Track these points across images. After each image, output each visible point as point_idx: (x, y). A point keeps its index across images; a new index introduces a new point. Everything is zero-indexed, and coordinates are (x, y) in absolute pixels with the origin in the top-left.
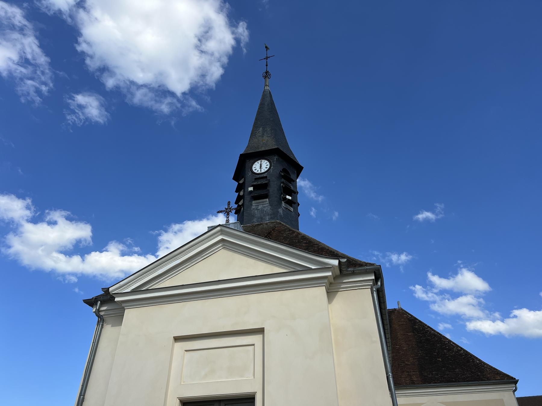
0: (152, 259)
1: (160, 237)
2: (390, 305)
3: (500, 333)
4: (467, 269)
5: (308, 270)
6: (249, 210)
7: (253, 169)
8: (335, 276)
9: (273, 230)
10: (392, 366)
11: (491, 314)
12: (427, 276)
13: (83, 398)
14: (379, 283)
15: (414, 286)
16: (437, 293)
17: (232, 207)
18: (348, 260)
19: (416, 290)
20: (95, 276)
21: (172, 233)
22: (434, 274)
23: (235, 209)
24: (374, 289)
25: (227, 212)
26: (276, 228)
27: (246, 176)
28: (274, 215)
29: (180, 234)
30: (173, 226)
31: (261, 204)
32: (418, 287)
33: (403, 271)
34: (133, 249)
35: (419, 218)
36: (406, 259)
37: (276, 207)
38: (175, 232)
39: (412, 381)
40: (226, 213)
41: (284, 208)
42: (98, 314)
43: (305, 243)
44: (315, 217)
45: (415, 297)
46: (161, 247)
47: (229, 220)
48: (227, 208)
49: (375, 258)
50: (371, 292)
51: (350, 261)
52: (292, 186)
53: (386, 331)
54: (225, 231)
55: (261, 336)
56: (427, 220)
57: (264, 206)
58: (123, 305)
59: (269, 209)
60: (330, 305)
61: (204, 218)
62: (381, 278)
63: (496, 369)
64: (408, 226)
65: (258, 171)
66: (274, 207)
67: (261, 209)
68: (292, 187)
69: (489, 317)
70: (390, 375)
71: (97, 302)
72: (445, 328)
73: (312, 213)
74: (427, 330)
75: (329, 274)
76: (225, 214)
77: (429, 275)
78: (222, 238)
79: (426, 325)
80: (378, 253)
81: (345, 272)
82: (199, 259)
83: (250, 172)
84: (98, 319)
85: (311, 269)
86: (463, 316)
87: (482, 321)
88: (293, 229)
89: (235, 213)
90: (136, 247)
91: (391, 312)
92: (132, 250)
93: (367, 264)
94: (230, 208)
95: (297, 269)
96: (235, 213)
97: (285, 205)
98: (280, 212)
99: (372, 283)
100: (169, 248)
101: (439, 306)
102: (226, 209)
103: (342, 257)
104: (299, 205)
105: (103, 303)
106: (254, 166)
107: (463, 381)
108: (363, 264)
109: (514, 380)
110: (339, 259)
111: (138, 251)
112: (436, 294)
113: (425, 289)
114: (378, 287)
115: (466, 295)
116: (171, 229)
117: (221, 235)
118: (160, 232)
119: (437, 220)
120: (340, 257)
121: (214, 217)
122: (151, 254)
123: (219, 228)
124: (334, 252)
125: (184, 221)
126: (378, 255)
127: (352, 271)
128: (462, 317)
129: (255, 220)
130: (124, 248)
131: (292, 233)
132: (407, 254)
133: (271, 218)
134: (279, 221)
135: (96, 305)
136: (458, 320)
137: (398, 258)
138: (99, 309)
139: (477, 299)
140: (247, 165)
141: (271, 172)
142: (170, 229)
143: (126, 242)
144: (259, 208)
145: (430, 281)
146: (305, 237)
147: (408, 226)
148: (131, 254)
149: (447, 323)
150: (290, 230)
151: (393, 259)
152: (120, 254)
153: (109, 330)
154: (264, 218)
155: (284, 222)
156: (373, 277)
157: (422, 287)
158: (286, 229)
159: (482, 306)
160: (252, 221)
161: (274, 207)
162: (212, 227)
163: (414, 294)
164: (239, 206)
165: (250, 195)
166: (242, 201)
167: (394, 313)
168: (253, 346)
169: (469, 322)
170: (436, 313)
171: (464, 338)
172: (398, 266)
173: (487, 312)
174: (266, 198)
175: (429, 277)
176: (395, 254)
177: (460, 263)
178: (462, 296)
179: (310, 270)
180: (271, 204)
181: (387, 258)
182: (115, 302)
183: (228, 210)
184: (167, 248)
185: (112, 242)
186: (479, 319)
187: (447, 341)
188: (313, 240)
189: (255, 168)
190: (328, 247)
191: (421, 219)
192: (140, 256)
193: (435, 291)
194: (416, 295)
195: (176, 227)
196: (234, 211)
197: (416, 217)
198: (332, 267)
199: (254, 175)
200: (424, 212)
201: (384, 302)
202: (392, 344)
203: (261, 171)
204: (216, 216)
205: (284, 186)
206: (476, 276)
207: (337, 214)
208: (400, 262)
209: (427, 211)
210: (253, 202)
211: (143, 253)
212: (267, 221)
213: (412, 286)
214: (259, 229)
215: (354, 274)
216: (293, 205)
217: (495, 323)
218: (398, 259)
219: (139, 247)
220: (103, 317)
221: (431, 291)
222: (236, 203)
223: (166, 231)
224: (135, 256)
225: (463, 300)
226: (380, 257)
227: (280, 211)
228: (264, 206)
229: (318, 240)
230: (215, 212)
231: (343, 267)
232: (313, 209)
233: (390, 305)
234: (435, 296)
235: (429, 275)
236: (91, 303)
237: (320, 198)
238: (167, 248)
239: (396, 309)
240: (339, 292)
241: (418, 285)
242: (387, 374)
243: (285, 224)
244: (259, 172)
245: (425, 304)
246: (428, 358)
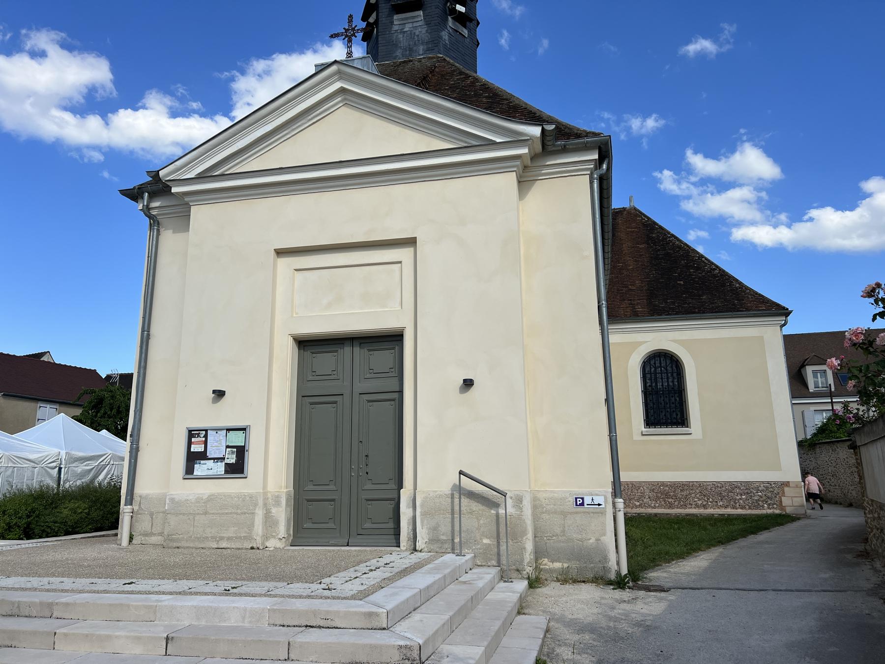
0: (224, 123)
1: (234, 84)
2: (618, 202)
3: (781, 244)
4: (752, 143)
5: (489, 144)
6: (388, 33)
8: (533, 155)
9: (431, 72)
10: (608, 293)
11: (773, 216)
12: (685, 154)
13: (148, 335)
14: (605, 166)
15: (661, 172)
16: (696, 182)
17: (356, 26)
18: (557, 128)
19: (663, 178)
20: (132, 152)
21: (254, 77)
22: (696, 152)
23: (362, 30)
24: (595, 176)
25: (348, 37)
26: (437, 70)
28: (434, 43)
29: (267, 79)
30: (255, 63)
31: (409, 21)
32: (667, 173)
33: (646, 147)
34: (189, 105)
35: (688, 51)
36: (654, 127)
37: (436, 27)
38: (259, 75)
39: (636, 312)
40: (347, 39)
41: (451, 30)
42: (148, 214)
43: (486, 97)
44: (508, 48)
45: (659, 190)
46: (237, 102)
47: (351, 52)
48: (347, 28)
49: (603, 125)
50: (590, 181)
51: (561, 128)
53: (606, 241)
54: (346, 72)
55: (412, 249)
56: (702, 56)
57: (415, 25)
58: (185, 199)
59: (424, 31)
60: (521, 202)
61: (308, 49)
62: (609, 157)
63: (762, 296)
64: (667, 67)
66: (432, 28)
67: (409, 32)
69: (769, 221)
70: (603, 304)
71: (143, 193)
72: (698, 237)
73: (503, 42)
74: (669, 240)
75: (525, 151)
76: (344, 39)
77: (689, 153)
78: (342, 87)
79: (669, 233)
80: (610, 116)
81: (550, 148)
82: (304, 123)
84: (150, 221)
85: (494, 143)
86: (730, 219)
87: (757, 226)
88: (468, 72)
89: (364, 39)
90: (195, 101)
91: (617, 213)
92: (188, 106)
93: (587, 134)
94: (353, 29)
95: (470, 144)
96: (364, 39)
97: (453, 23)
98: (444, 37)
99: (592, 166)
100: (251, 105)
101: (695, 204)
102: (347, 30)
103: (547, 122)
104: (478, 23)
105: (153, 195)
107: (709, 313)
108: (581, 134)
109: (787, 311)
110: (542, 125)
111: (199, 110)
112: (694, 184)
113: (675, 177)
114: (601, 173)
115: (741, 185)
116: (251, 70)
117: (340, 79)
118: (232, 74)
119: (719, 55)
120: (544, 121)
121: (325, 48)
122: (222, 115)
123: (334, 68)
124: (535, 113)
125: (273, 55)
126: (609, 119)
127: (562, 147)
128: (728, 221)
129: (399, 53)
130: (174, 104)
131: (465, 78)
132: (657, 118)
133: (428, 50)
134: (441, 56)
135: (143, 198)
136: (720, 226)
137: (642, 124)
138: (147, 206)
139: (758, 192)
142: (249, 68)
143: (176, 92)
144: (405, 30)
145: (689, 164)
146: (487, 86)
147: (667, 67)
148: (187, 113)
149: (701, 229)
150: (461, 73)
151: (633, 126)
152: (168, 113)
153: (169, 239)
154: (415, 48)
155: (450, 58)
156: (596, 156)
157: (674, 173)
158: (454, 71)
159: (763, 203)
160: (394, 55)
161: (432, 28)
162: (323, 64)
163: (659, 185)
164: (369, 24)
165: (389, 3)
166: (374, 15)
167: (622, 214)
168: (400, 265)
169: (736, 227)
170: (688, 215)
171: (723, 252)
172: (641, 137)
173: (769, 212)
174: (420, 10)
175: (687, 157)
176: (637, 118)
177: (743, 132)
178: (734, 188)
179: (492, 144)
180: (428, 24)
181: (623, 124)
182: (173, 194)
183: (350, 33)
184: (249, 104)
185: (150, 92)
186: (753, 223)
187: (698, 255)
188: (501, 91)
190: (526, 104)
191: (691, 54)
192: (203, 118)
193: (693, 179)
194: (662, 187)
195: (260, 65)
196: (360, 35)
197: (683, 50)
198: (530, 139)
200: (699, 40)
201: (609, 197)
202: (612, 261)
204: (329, 45)
206: (764, 155)
207: (546, 43)
208: (643, 131)
209: (705, 37)
210: (396, 17)
211: (208, 113)
212: (420, 55)
213: (657, 171)
214: (406, 70)
215: (564, 150)
216: (468, 23)
217: (778, 230)
218: (642, 126)
219: (199, 103)
220: (156, 218)
221: (687, 180)
222: (365, 18)
223: (243, 72)
224: (193, 117)
225: (736, 194)
226: (611, 123)
227: (445, 35)
228: (415, 25)
229: (508, 92)
230: (328, 38)
231: (548, 138)
232: (506, 33)
233: (618, 202)
234: (692, 187)
235: (689, 153)
236: (134, 195)
237: (518, 11)
238: (249, 104)
239: (626, 208)
240: (538, 181)
241: (668, 170)
242: (599, 303)
243: (452, 61)
245: (674, 200)
246: (663, 280)
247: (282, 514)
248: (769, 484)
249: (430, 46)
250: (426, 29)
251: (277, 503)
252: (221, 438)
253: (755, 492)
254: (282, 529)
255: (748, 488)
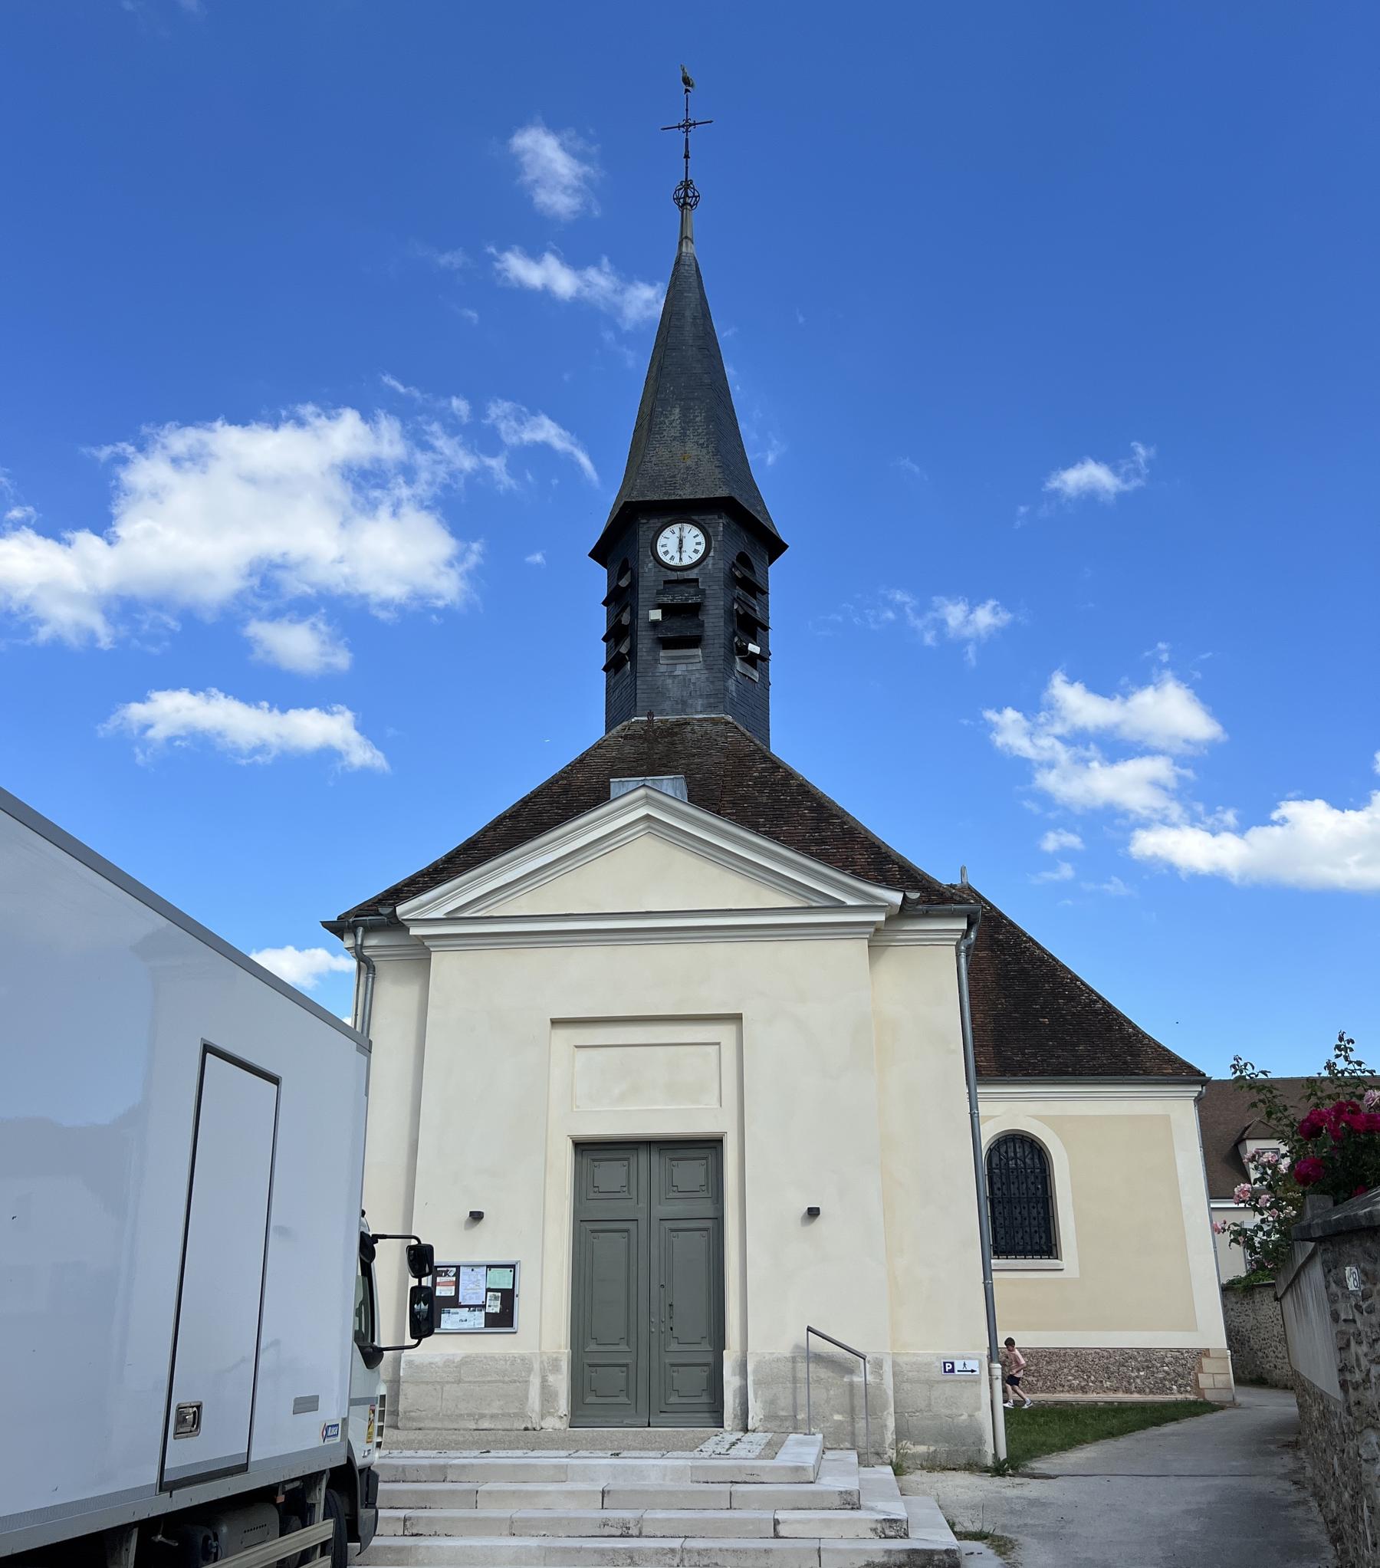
7: (660, 551)
27: (641, 570)
52: (759, 604)
65: (672, 558)
66: (715, 675)
68: (757, 608)
83: (652, 558)
106: (661, 541)
140: (641, 533)
141: (710, 567)
161: (715, 675)
174: (696, 647)
180: (709, 668)
189: (664, 549)
199: (663, 569)
203: (681, 559)
205: (741, 613)
227: (731, 684)
228: (691, 667)
244: (676, 562)
247: (561, 1382)
248: (1179, 1352)
249: (712, 700)
250: (707, 675)
251: (555, 1367)
252: (479, 1277)
253: (1159, 1365)
254: (563, 1405)
255: (1147, 1358)
